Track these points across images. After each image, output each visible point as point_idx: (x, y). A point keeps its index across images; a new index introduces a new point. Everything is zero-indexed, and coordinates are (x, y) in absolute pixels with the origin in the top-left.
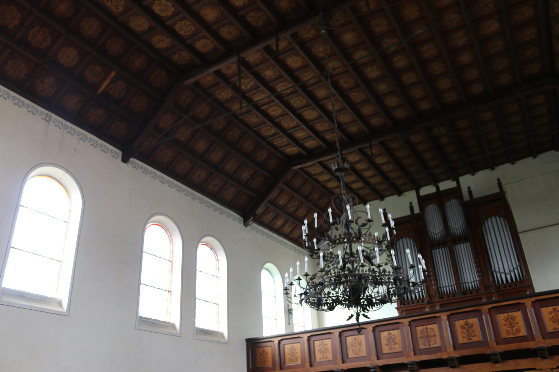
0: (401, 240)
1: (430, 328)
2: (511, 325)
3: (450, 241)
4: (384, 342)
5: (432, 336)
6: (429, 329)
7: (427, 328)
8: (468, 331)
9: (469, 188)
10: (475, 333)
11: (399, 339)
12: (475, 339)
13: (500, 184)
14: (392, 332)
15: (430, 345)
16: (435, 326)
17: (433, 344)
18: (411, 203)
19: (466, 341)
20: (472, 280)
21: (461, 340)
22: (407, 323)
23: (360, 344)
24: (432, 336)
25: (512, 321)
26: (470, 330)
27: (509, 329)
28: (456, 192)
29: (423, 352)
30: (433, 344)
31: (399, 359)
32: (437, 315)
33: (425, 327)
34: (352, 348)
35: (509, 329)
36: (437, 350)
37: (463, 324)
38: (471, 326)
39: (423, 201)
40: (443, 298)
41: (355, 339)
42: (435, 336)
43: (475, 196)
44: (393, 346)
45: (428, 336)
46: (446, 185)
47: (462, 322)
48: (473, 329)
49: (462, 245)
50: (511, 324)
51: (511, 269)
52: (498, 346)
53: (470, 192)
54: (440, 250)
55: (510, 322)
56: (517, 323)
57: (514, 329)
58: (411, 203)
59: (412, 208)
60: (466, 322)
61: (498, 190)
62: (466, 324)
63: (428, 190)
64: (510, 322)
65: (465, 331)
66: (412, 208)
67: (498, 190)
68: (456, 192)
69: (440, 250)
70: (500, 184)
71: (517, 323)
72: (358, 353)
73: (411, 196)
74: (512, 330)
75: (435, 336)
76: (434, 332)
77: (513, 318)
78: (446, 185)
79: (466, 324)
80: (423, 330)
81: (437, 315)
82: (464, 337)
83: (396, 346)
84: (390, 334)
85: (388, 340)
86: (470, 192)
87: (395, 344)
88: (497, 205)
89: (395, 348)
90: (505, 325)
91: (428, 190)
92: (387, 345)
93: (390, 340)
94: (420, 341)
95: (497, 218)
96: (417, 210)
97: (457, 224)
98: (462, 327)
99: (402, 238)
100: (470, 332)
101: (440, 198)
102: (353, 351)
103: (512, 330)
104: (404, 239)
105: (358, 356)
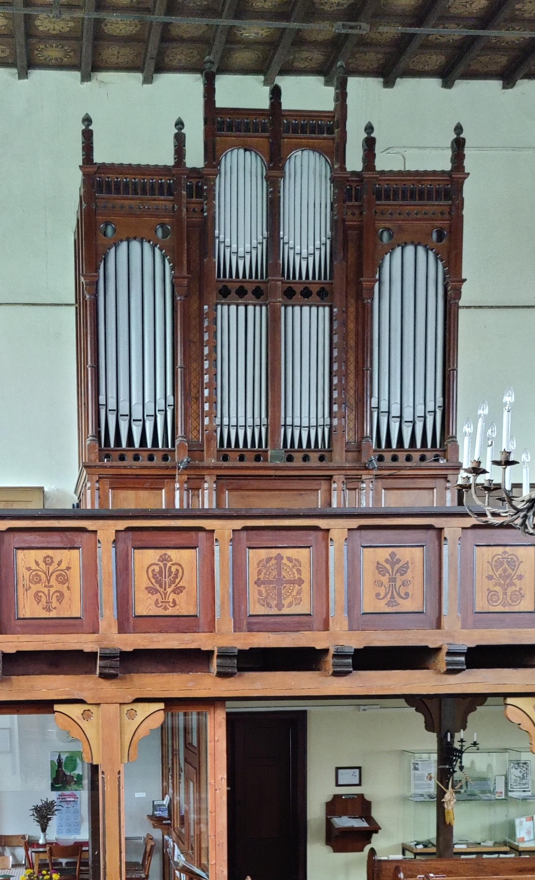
0: (124, 245)
1: (289, 559)
2: (507, 580)
3: (272, 287)
4: (141, 580)
5: (292, 582)
6: (285, 561)
7: (279, 558)
8: (393, 580)
9: (369, 128)
10: (410, 590)
11: (190, 579)
12: (407, 605)
13: (459, 145)
14: (172, 553)
15: (280, 606)
16: (303, 555)
17: (290, 605)
18: (180, 124)
19: (382, 606)
20: (313, 422)
21: (368, 603)
22: (229, 534)
23: (64, 579)
24: (292, 582)
25: (510, 571)
26: (399, 580)
27: (497, 588)
28: (325, 131)
29: (255, 624)
30: (290, 605)
31: (187, 637)
32: (322, 523)
33: (274, 552)
34: (35, 588)
35: (497, 588)
36: (301, 622)
37: (382, 562)
38: (403, 570)
39: (222, 126)
40: (225, 458)
41: (49, 561)
42: (300, 582)
43: (382, 163)
44: (172, 596)
45: (279, 581)
46: (307, 93)
47: (383, 554)
48: (408, 576)
49: (306, 309)
50: (506, 576)
51: (420, 411)
52: (465, 631)
53: (370, 144)
54: (233, 308)
55: (505, 571)
56: (520, 577)
57: (509, 590)
58: (180, 124)
59: (180, 141)
60: (393, 555)
61: (444, 163)
62: (393, 561)
63: (241, 92)
64: (505, 571)
65: (385, 579)
66: (180, 141)
67: (444, 163)
68: (325, 131)
69: (233, 308)
70: (459, 145)
71: (520, 577)
72: (55, 603)
73: (179, 95)
74: (505, 594)
75: (300, 582)
76: (299, 571)
77: (513, 563)
78: (307, 93)
79: (393, 561)
80: (269, 560)
81: (322, 523)
82: (378, 595)
83: (181, 598)
84: (164, 559)
85: (158, 577)
86: (370, 144)
87: (178, 590)
88: (431, 207)
89: (174, 602)
90: (490, 578)
91: (241, 92)
92: (151, 590)
93: (165, 580)
94: (253, 592)
95: (421, 250)
96: (195, 158)
97: (307, 239)
98: (379, 567)
99: (128, 240)
100: (398, 583)
101: (274, 134)
102: (37, 596)
103: (505, 594)
104: (135, 245)
105: (53, 614)
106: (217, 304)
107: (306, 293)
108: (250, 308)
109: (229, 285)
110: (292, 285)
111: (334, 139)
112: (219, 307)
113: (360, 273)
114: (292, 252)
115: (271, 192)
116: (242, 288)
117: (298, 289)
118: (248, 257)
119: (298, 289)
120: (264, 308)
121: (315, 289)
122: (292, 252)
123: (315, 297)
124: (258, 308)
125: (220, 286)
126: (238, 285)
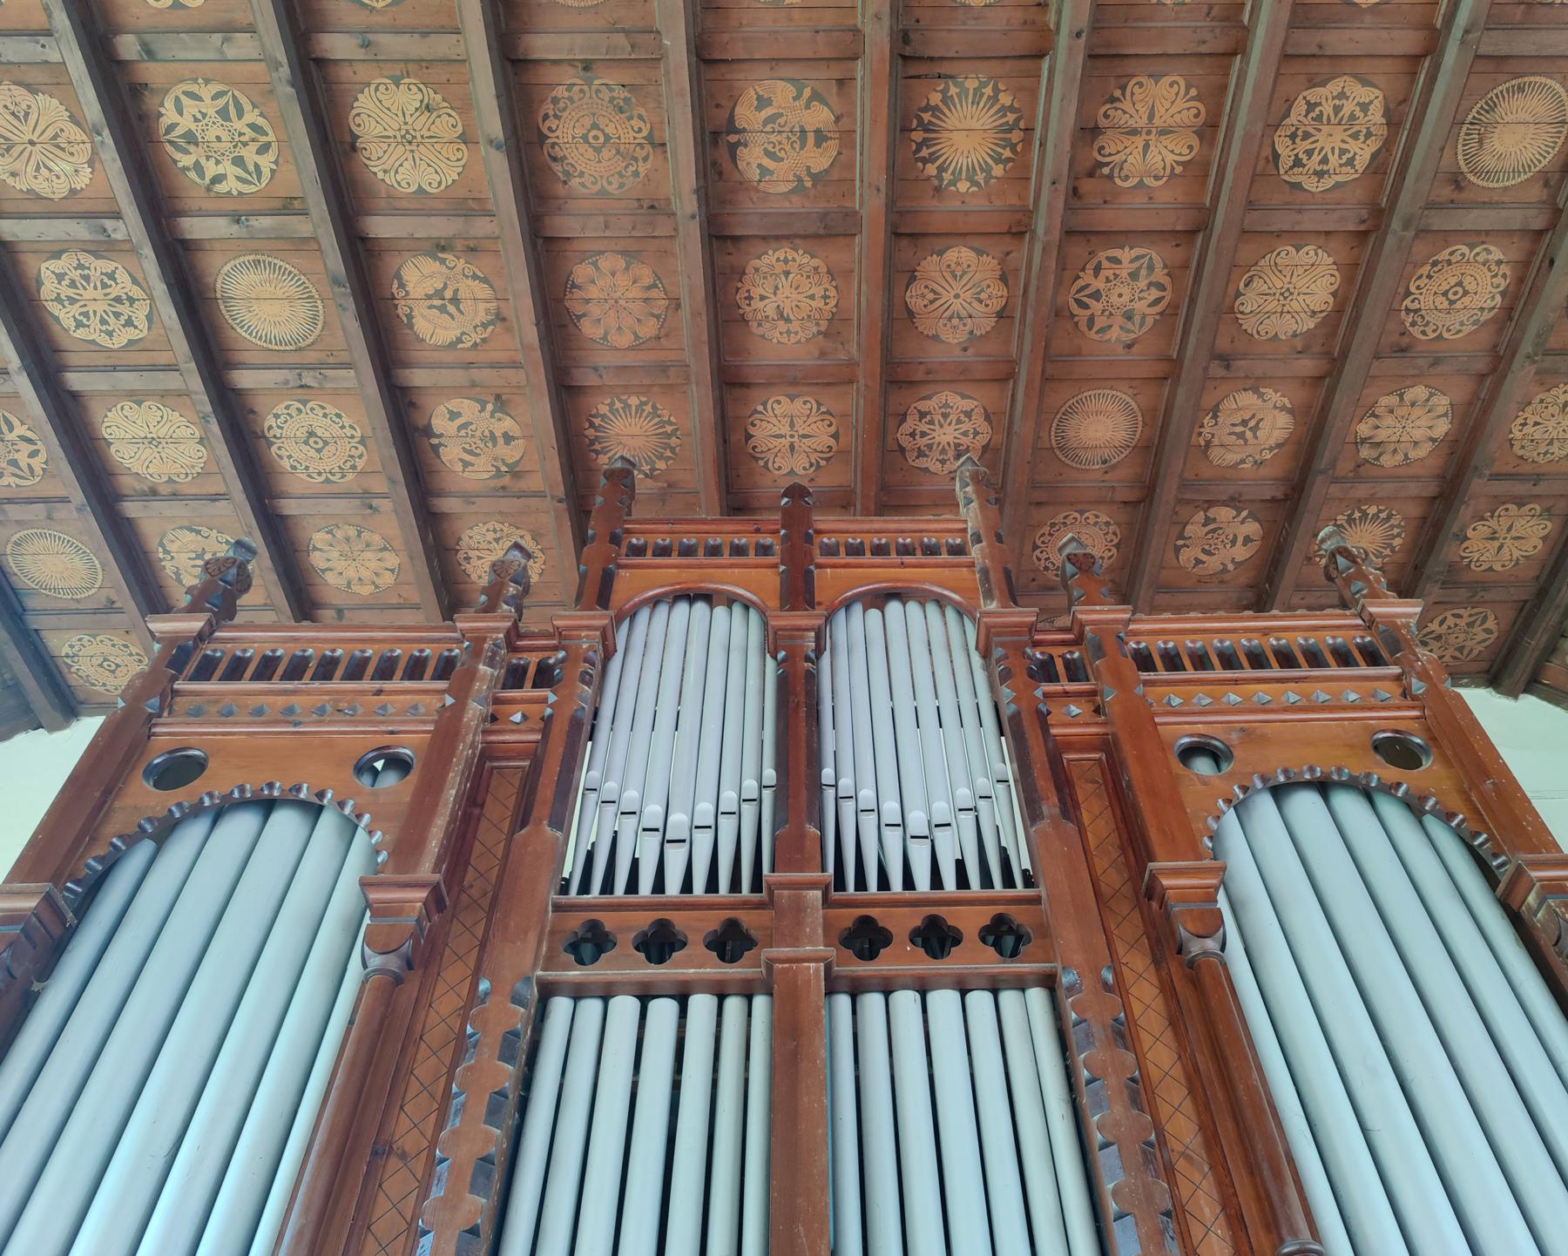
49: (944, 1001)
106: (548, 991)
107: (936, 937)
108: (701, 1005)
109: (609, 921)
110: (873, 912)
111: (972, 565)
112: (561, 1006)
113: (1135, 846)
114: (868, 822)
115: (784, 660)
116: (663, 926)
117: (901, 923)
118: (703, 842)
119: (901, 923)
120: (760, 1002)
121: (970, 921)
122: (868, 822)
123: (974, 958)
124: (734, 1005)
125: (575, 922)
126: (645, 920)
